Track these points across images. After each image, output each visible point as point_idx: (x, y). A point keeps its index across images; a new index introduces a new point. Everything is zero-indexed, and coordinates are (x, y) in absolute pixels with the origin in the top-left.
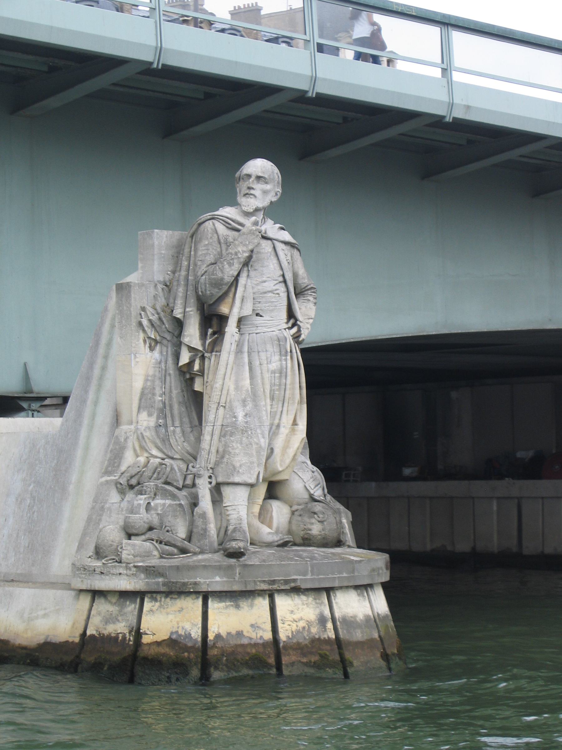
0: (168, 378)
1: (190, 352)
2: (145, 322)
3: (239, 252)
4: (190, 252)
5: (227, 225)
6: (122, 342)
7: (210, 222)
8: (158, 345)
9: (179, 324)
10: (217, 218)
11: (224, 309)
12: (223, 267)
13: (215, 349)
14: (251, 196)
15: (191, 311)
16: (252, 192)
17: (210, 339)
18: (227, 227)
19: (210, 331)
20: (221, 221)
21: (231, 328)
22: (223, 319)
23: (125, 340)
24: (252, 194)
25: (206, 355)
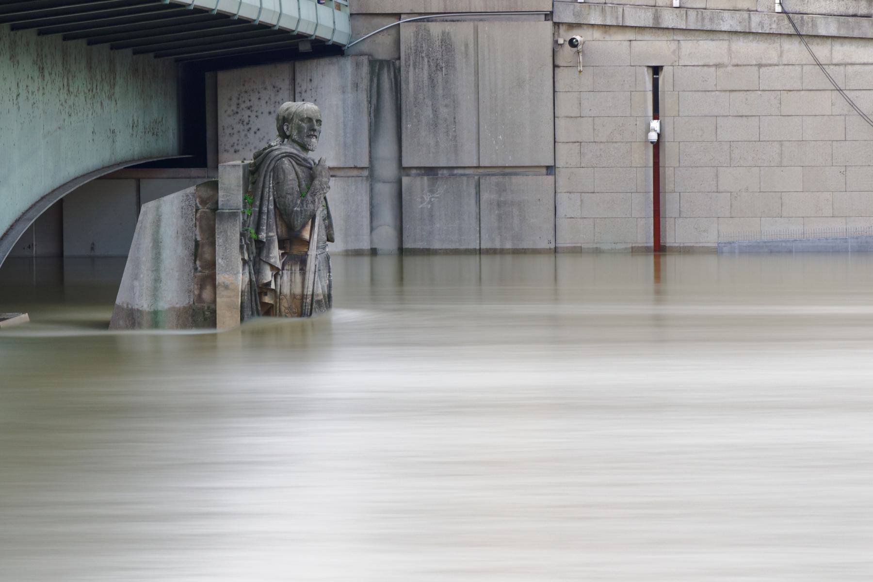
0: (253, 293)
1: (271, 271)
2: (245, 246)
3: (324, 188)
4: (270, 184)
5: (298, 162)
6: (224, 262)
7: (286, 158)
8: (247, 265)
9: (261, 246)
10: (294, 157)
11: (306, 235)
12: (314, 201)
13: (285, 268)
14: (314, 137)
15: (274, 236)
16: (316, 134)
17: (282, 259)
18: (297, 164)
19: (281, 252)
20: (293, 158)
21: (313, 252)
22: (307, 243)
24: (315, 136)
25: (281, 273)
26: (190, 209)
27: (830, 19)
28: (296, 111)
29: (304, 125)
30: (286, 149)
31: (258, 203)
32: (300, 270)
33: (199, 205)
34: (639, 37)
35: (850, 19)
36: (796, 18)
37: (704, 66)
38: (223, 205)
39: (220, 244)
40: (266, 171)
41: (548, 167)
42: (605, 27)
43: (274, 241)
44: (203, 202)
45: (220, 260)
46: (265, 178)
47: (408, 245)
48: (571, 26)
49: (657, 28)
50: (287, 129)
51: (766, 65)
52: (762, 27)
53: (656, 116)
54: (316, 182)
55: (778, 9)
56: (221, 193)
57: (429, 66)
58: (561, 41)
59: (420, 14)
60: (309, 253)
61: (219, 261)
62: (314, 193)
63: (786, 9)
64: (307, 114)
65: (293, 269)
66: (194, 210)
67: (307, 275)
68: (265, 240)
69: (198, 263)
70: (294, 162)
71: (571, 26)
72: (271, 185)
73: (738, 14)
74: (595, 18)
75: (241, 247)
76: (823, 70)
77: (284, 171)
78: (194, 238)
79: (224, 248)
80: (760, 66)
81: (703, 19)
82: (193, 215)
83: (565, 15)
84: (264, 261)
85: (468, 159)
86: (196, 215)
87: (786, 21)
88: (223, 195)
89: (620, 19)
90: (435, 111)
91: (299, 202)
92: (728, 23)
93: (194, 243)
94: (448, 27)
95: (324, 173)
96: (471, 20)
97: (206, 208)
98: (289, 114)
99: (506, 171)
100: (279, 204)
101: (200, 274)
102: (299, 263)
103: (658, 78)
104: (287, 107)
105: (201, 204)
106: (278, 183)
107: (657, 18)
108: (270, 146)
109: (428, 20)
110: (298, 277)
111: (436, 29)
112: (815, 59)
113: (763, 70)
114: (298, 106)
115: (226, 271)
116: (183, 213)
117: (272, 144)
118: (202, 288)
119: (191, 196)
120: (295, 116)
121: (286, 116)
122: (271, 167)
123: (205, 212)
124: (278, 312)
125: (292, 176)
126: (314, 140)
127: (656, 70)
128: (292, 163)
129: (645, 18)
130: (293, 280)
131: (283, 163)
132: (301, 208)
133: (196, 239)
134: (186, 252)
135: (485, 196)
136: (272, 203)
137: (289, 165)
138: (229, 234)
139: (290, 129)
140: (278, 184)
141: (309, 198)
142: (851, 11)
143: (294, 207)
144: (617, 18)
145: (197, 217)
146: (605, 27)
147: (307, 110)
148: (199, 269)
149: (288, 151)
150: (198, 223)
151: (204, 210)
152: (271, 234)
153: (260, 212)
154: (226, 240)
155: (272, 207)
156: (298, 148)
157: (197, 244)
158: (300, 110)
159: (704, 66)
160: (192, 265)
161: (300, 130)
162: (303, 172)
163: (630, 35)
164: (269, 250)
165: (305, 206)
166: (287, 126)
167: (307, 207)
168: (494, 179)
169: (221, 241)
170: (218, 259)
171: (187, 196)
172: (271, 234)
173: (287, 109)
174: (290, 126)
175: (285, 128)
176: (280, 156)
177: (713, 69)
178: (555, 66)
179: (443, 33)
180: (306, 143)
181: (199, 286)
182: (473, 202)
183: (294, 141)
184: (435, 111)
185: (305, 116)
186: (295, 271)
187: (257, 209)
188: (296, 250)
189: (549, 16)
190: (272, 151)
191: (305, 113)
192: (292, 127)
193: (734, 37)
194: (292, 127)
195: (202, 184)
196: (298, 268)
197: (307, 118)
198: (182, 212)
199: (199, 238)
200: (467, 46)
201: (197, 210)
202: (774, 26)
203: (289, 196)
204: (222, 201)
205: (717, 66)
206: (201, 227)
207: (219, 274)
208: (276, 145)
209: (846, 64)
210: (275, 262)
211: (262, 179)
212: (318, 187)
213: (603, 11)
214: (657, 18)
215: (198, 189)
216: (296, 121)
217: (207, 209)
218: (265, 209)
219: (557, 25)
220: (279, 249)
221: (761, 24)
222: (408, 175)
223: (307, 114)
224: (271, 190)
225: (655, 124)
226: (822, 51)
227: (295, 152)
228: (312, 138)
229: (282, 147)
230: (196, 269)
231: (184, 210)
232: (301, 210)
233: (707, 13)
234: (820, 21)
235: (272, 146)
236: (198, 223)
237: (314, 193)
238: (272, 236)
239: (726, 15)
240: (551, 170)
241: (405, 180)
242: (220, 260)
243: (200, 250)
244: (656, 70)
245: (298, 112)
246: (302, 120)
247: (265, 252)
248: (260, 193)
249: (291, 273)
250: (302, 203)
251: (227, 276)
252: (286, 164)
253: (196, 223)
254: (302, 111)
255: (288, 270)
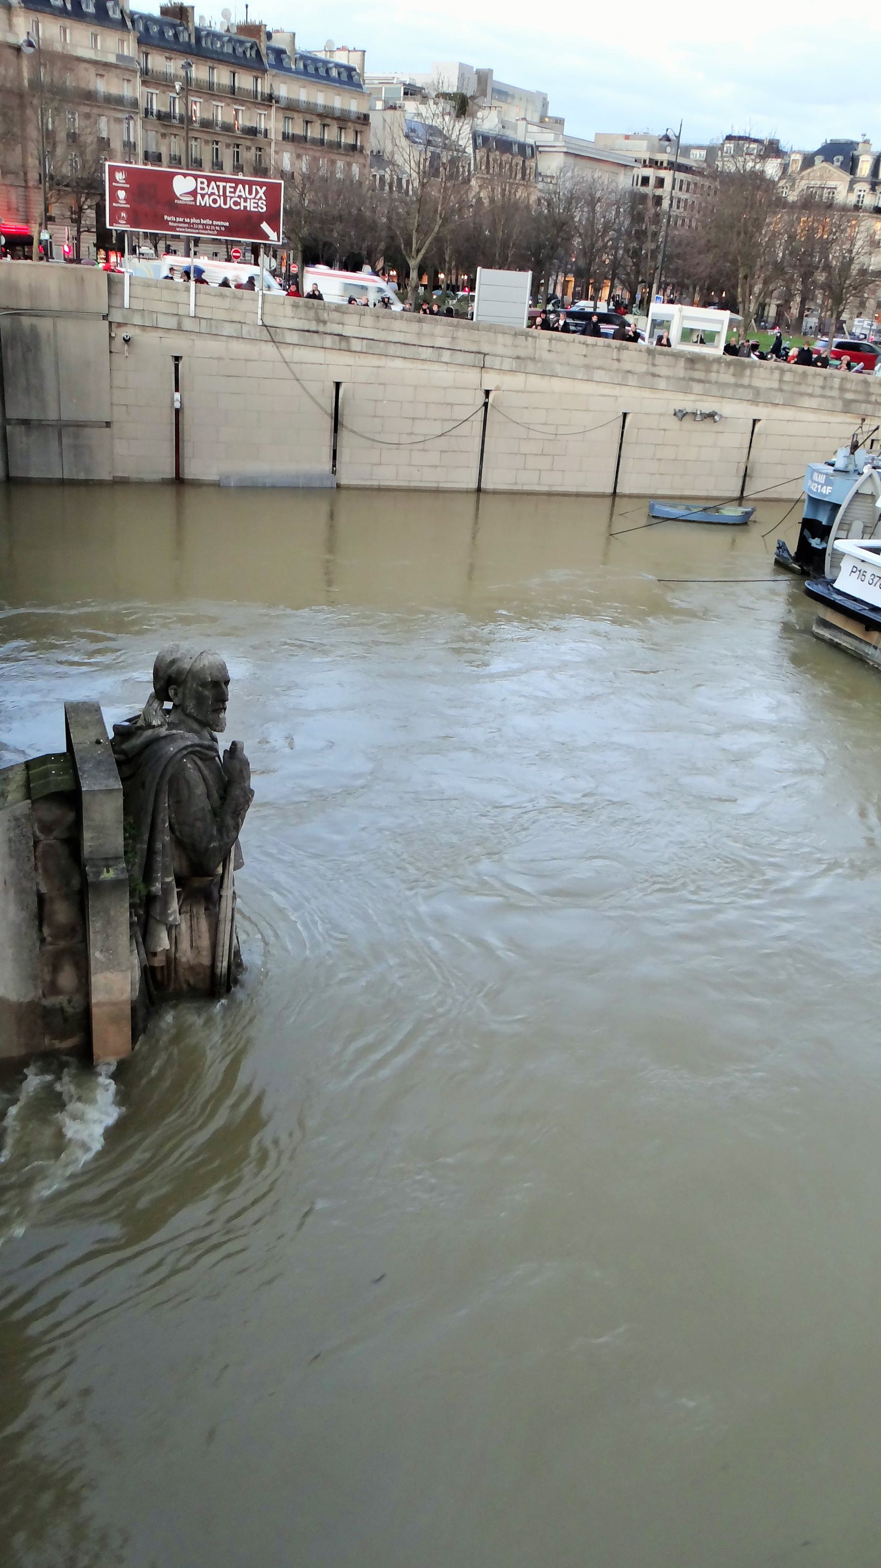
6: (104, 956)
9: (149, 900)
18: (201, 759)
23: (111, 954)
26: (24, 842)
27: (294, 332)
28: (190, 669)
29: (207, 693)
30: (182, 738)
31: (146, 837)
32: (206, 910)
33: (38, 833)
34: (166, 335)
35: (306, 333)
36: (272, 330)
37: (210, 358)
38: (91, 852)
39: (97, 930)
40: (158, 784)
41: (106, 422)
42: (143, 327)
43: (172, 889)
44: (46, 829)
45: (98, 954)
46: (157, 795)
47: (13, 473)
48: (120, 325)
49: (180, 329)
50: (176, 694)
51: (252, 361)
52: (250, 335)
53: (177, 390)
54: (236, 792)
55: (260, 323)
56: (87, 835)
57: (22, 347)
58: (113, 335)
59: (13, 309)
60: (224, 893)
61: (96, 955)
62: (237, 813)
63: (267, 323)
64: (211, 674)
65: (195, 911)
66: (32, 843)
67: (221, 927)
68: (160, 893)
69: (46, 931)
70: (199, 762)
71: (120, 325)
72: (166, 805)
73: (234, 325)
74: (137, 320)
75: (132, 924)
76: (288, 366)
77: (188, 783)
78: (35, 888)
79: (105, 935)
80: (247, 360)
81: (211, 327)
82: (30, 852)
83: (117, 317)
84: (155, 919)
85: (52, 415)
86: (35, 851)
87: (266, 331)
88: (92, 838)
89: (155, 322)
90: (28, 380)
91: (215, 832)
92: (228, 329)
93: (36, 898)
94: (35, 321)
95: (245, 773)
96: (50, 316)
97: (52, 838)
98: (179, 672)
99: (79, 425)
100: (180, 832)
101: (51, 947)
102: (203, 901)
103: (178, 364)
104: (173, 658)
105: (41, 832)
106: (178, 802)
107: (179, 324)
108: (150, 726)
109: (19, 314)
110: (204, 925)
111: (26, 321)
112: (283, 358)
113: (249, 363)
114: (193, 660)
115: (108, 969)
116: (13, 848)
117: (154, 723)
118: (55, 969)
119: (23, 820)
120: (189, 679)
121: (174, 676)
122: (167, 778)
123: (51, 846)
124: (173, 975)
125: (200, 790)
126: (222, 715)
127: (177, 359)
128: (196, 764)
129: (172, 323)
130: (195, 927)
131: (183, 768)
132: (219, 841)
133: (38, 891)
134: (23, 914)
135: (65, 441)
136: (168, 831)
137: (194, 769)
138: (112, 913)
139: (180, 695)
140: (178, 803)
141: (229, 821)
142: (306, 328)
143: (210, 842)
144: (153, 321)
145: (37, 853)
146: (143, 327)
147: (211, 667)
148: (49, 939)
149: (189, 743)
150: (39, 864)
151: (48, 842)
152: (168, 880)
153: (151, 852)
154: (108, 922)
155: (167, 838)
156: (196, 726)
157: (41, 899)
158: (199, 665)
159: (210, 358)
160: (35, 935)
161: (200, 700)
162: (210, 770)
163: (160, 333)
164: (166, 904)
165: (225, 837)
166: (175, 690)
167: (228, 838)
168: (71, 429)
169: (98, 925)
170: (94, 954)
171: (17, 819)
172: (168, 880)
173: (173, 662)
174: (180, 690)
175: (171, 693)
176: (179, 756)
177: (216, 361)
178: (111, 352)
179: (32, 325)
180: (211, 722)
181: (51, 968)
182: (56, 444)
183: (189, 716)
184: (28, 380)
185: (210, 680)
186: (198, 913)
187: (145, 846)
188: (197, 883)
189: (105, 317)
190: (158, 739)
191: (208, 672)
192: (184, 694)
193: (230, 339)
194: (184, 694)
195: (41, 798)
196: (203, 911)
197: (212, 681)
198: (10, 847)
199: (44, 889)
200: (49, 335)
201: (36, 843)
202: (258, 334)
203: (199, 824)
204: (90, 846)
205: (218, 359)
206: (45, 870)
207: (96, 973)
208: (161, 726)
209: (301, 363)
210: (175, 919)
211: (152, 798)
212: (242, 800)
213: (143, 316)
214: (179, 324)
215: (35, 807)
216: (193, 685)
217: (55, 838)
218: (159, 846)
219: (110, 323)
220: (177, 887)
221: (249, 332)
222: (9, 424)
223: (211, 674)
224: (167, 812)
225: (177, 396)
226: (287, 352)
227: (197, 740)
228: (219, 713)
229: (174, 731)
230: (43, 940)
231: (13, 844)
232: (220, 845)
233: (214, 322)
234: (287, 333)
235: (154, 727)
236: (39, 864)
237: (237, 813)
238: (169, 883)
239: (226, 325)
240: (108, 424)
241: (8, 428)
242: (98, 954)
243: (47, 908)
244: (177, 359)
245: (194, 669)
246: (204, 685)
247: (157, 908)
248: (149, 820)
249: (191, 916)
250: (220, 831)
251: (109, 975)
252: (190, 768)
253: (36, 864)
254: (203, 669)
255: (187, 913)
